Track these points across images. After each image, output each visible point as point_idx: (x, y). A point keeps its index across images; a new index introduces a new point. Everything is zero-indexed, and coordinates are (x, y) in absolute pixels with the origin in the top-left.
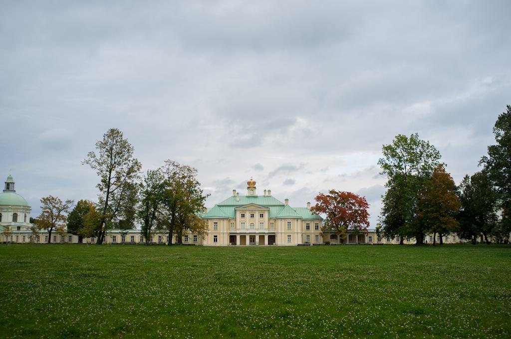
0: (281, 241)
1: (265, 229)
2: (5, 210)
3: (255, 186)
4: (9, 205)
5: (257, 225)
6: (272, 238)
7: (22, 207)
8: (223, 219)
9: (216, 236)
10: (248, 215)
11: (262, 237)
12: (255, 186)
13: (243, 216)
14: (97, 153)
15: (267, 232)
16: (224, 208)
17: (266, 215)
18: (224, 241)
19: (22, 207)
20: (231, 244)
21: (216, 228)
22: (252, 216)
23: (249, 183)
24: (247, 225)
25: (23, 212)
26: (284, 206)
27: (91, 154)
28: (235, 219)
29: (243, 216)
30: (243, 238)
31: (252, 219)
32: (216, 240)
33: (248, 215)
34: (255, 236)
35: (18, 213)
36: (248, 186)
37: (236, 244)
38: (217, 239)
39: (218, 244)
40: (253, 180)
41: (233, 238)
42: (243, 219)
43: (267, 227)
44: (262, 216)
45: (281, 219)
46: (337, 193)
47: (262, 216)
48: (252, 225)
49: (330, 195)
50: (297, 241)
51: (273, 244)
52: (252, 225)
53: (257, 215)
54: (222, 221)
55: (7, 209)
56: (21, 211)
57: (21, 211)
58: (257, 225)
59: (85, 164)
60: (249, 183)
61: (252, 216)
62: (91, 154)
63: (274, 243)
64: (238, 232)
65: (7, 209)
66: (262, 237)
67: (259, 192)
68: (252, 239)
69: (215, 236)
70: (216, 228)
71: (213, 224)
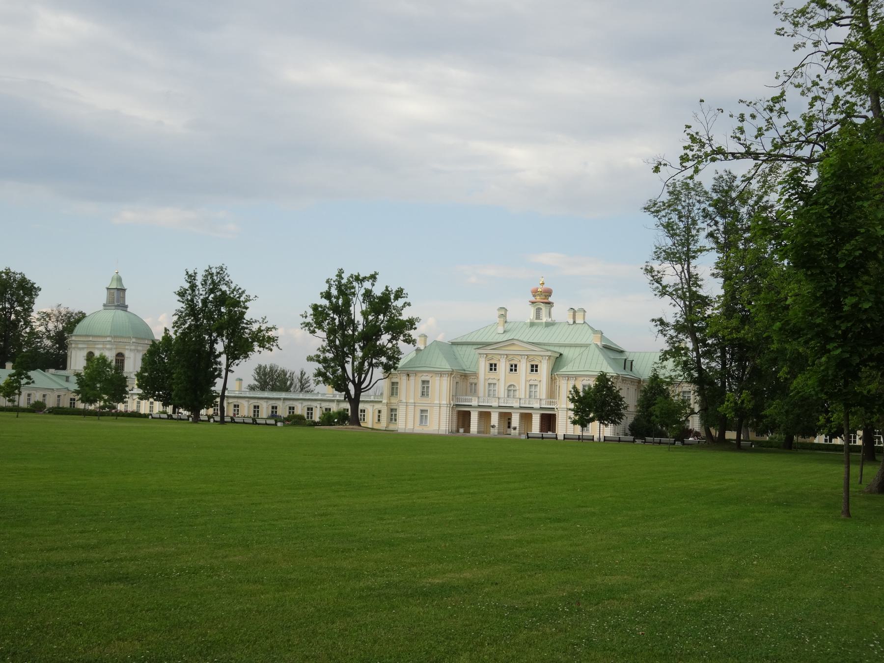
1: (539, 402)
2: (101, 346)
3: (550, 299)
4: (122, 337)
5: (522, 391)
6: (549, 421)
7: (134, 340)
8: (441, 374)
10: (503, 366)
11: (526, 418)
12: (550, 299)
13: (493, 367)
16: (464, 347)
18: (440, 423)
19: (134, 340)
21: (424, 393)
22: (514, 368)
23: (535, 293)
24: (501, 390)
25: (138, 351)
26: (587, 346)
28: (475, 374)
29: (493, 367)
30: (485, 416)
33: (503, 366)
34: (510, 414)
35: (127, 354)
36: (533, 299)
38: (426, 416)
40: (546, 286)
41: (463, 418)
42: (492, 375)
43: (544, 396)
44: (534, 368)
48: (511, 389)
52: (511, 389)
53: (523, 367)
55: (104, 343)
56: (133, 347)
57: (101, 346)
58: (522, 391)
60: (535, 293)
61: (514, 368)
64: (474, 403)
65: (104, 343)
66: (526, 418)
67: (560, 312)
68: (506, 418)
69: (422, 411)
70: (424, 393)
71: (420, 383)
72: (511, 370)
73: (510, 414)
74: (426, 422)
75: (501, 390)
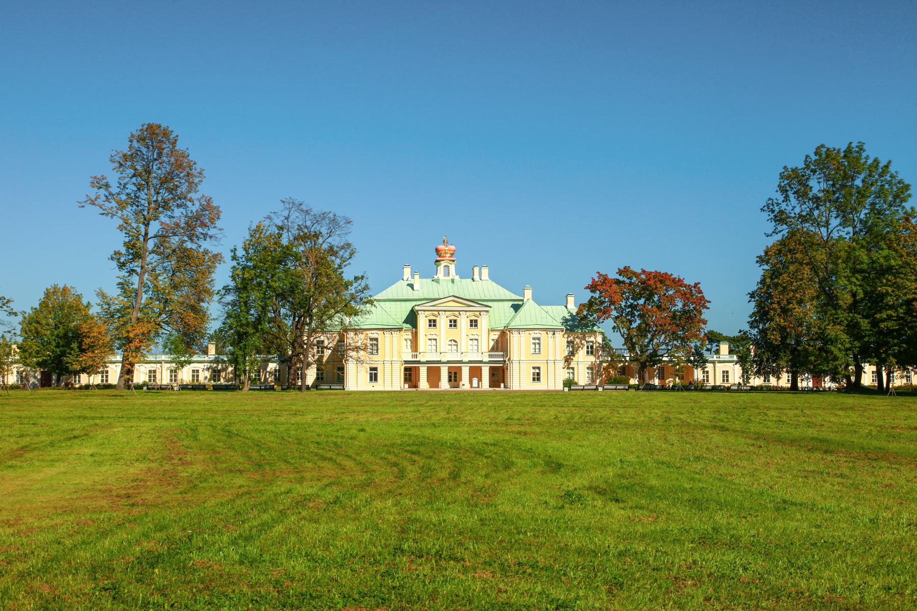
0: (520, 380)
5: (465, 344)
6: (499, 375)
9: (375, 369)
10: (443, 321)
13: (433, 323)
14: (114, 179)
15: (486, 359)
17: (484, 322)
18: (392, 381)
20: (406, 386)
22: (453, 324)
24: (444, 345)
27: (100, 183)
31: (453, 330)
32: (374, 377)
33: (443, 321)
37: (416, 386)
38: (376, 375)
39: (378, 387)
41: (410, 374)
42: (433, 330)
44: (474, 323)
45: (519, 330)
46: (637, 275)
47: (474, 323)
49: (621, 278)
50: (554, 380)
51: (499, 387)
54: (387, 334)
59: (89, 207)
61: (453, 324)
62: (100, 183)
63: (502, 385)
66: (475, 372)
69: (372, 369)
72: (451, 326)
73: (460, 367)
74: (376, 380)
75: (444, 345)
